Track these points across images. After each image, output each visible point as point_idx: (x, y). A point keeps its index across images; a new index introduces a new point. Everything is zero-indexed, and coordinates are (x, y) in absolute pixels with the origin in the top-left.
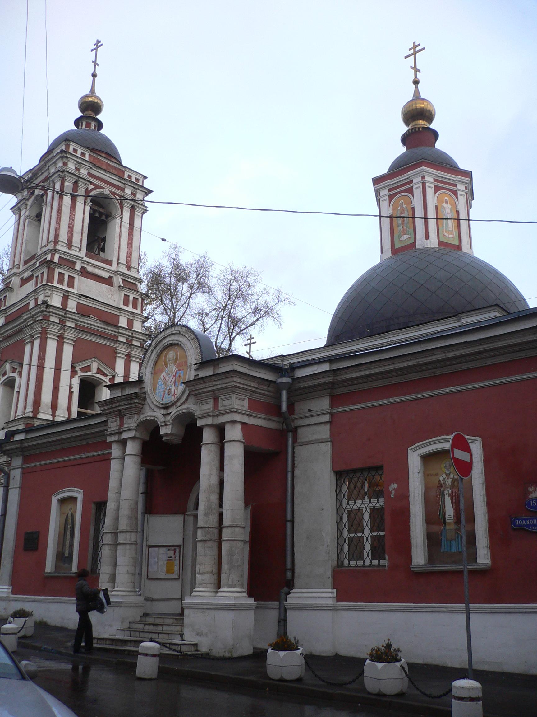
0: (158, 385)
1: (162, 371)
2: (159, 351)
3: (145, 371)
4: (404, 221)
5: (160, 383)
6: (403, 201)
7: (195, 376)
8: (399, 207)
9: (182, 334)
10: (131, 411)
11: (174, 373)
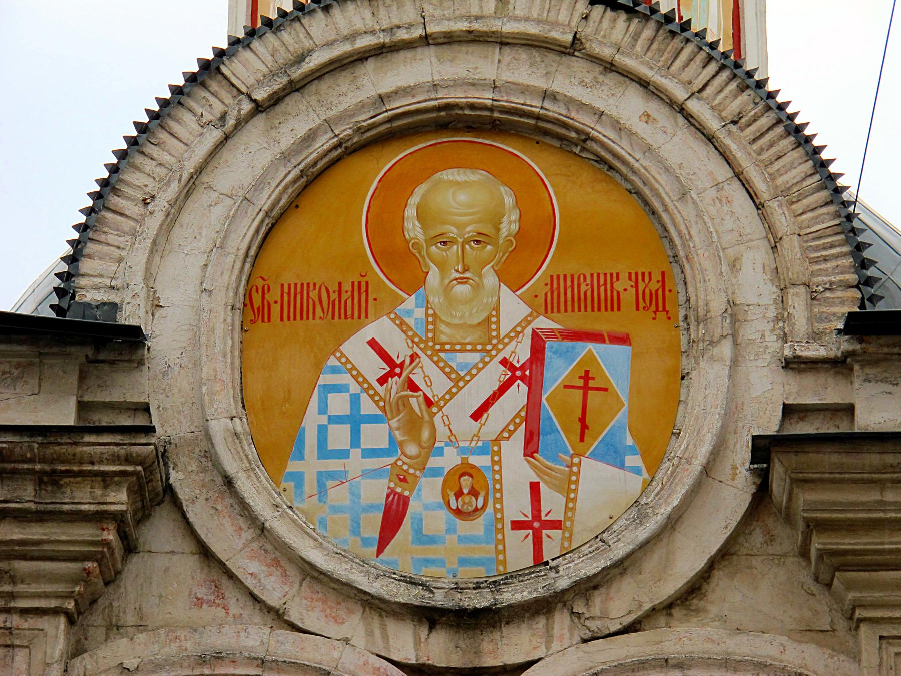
0: (312, 420)
2: (324, 142)
3: (149, 276)
7: (789, 411)
9: (594, 59)
10: (13, 580)
11: (521, 352)
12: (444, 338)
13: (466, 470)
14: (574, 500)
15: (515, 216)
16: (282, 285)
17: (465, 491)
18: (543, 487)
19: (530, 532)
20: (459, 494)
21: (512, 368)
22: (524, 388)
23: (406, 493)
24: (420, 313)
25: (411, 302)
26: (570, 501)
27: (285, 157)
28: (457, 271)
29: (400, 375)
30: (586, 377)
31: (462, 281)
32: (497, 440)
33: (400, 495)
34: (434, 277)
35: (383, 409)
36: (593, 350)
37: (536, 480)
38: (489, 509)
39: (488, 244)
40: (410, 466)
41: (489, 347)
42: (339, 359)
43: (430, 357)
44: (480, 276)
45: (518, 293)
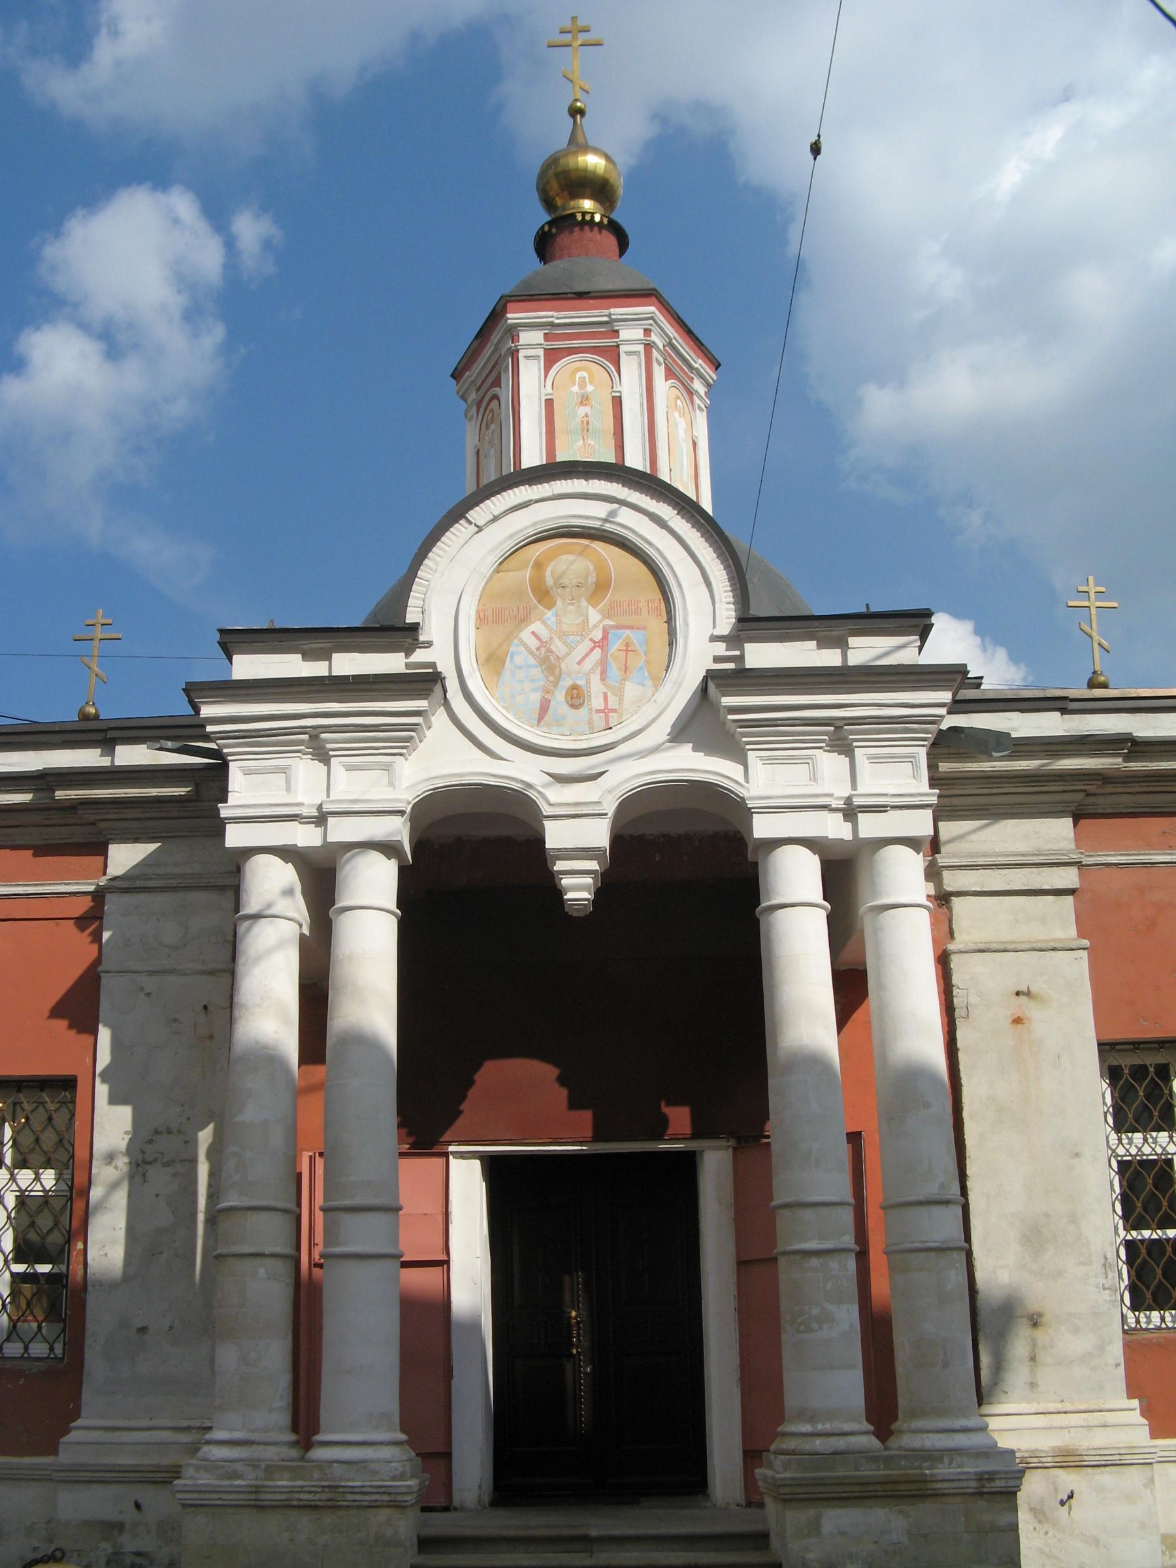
1: (523, 619)
4: (588, 423)
5: (518, 660)
6: (585, 374)
8: (575, 385)
11: (598, 635)
12: (565, 630)
13: (575, 687)
14: (623, 700)
15: (594, 575)
16: (493, 609)
17: (575, 696)
18: (609, 694)
19: (603, 714)
20: (572, 698)
21: (595, 642)
22: (600, 650)
23: (550, 698)
24: (554, 619)
25: (549, 614)
26: (621, 700)
27: (491, 551)
28: (570, 600)
29: (545, 647)
30: (627, 645)
31: (573, 604)
32: (588, 674)
33: (546, 698)
34: (559, 603)
35: (538, 662)
36: (631, 635)
37: (605, 691)
38: (586, 704)
39: (582, 587)
40: (551, 686)
41: (584, 633)
42: (518, 640)
43: (559, 638)
44: (579, 602)
45: (597, 608)
